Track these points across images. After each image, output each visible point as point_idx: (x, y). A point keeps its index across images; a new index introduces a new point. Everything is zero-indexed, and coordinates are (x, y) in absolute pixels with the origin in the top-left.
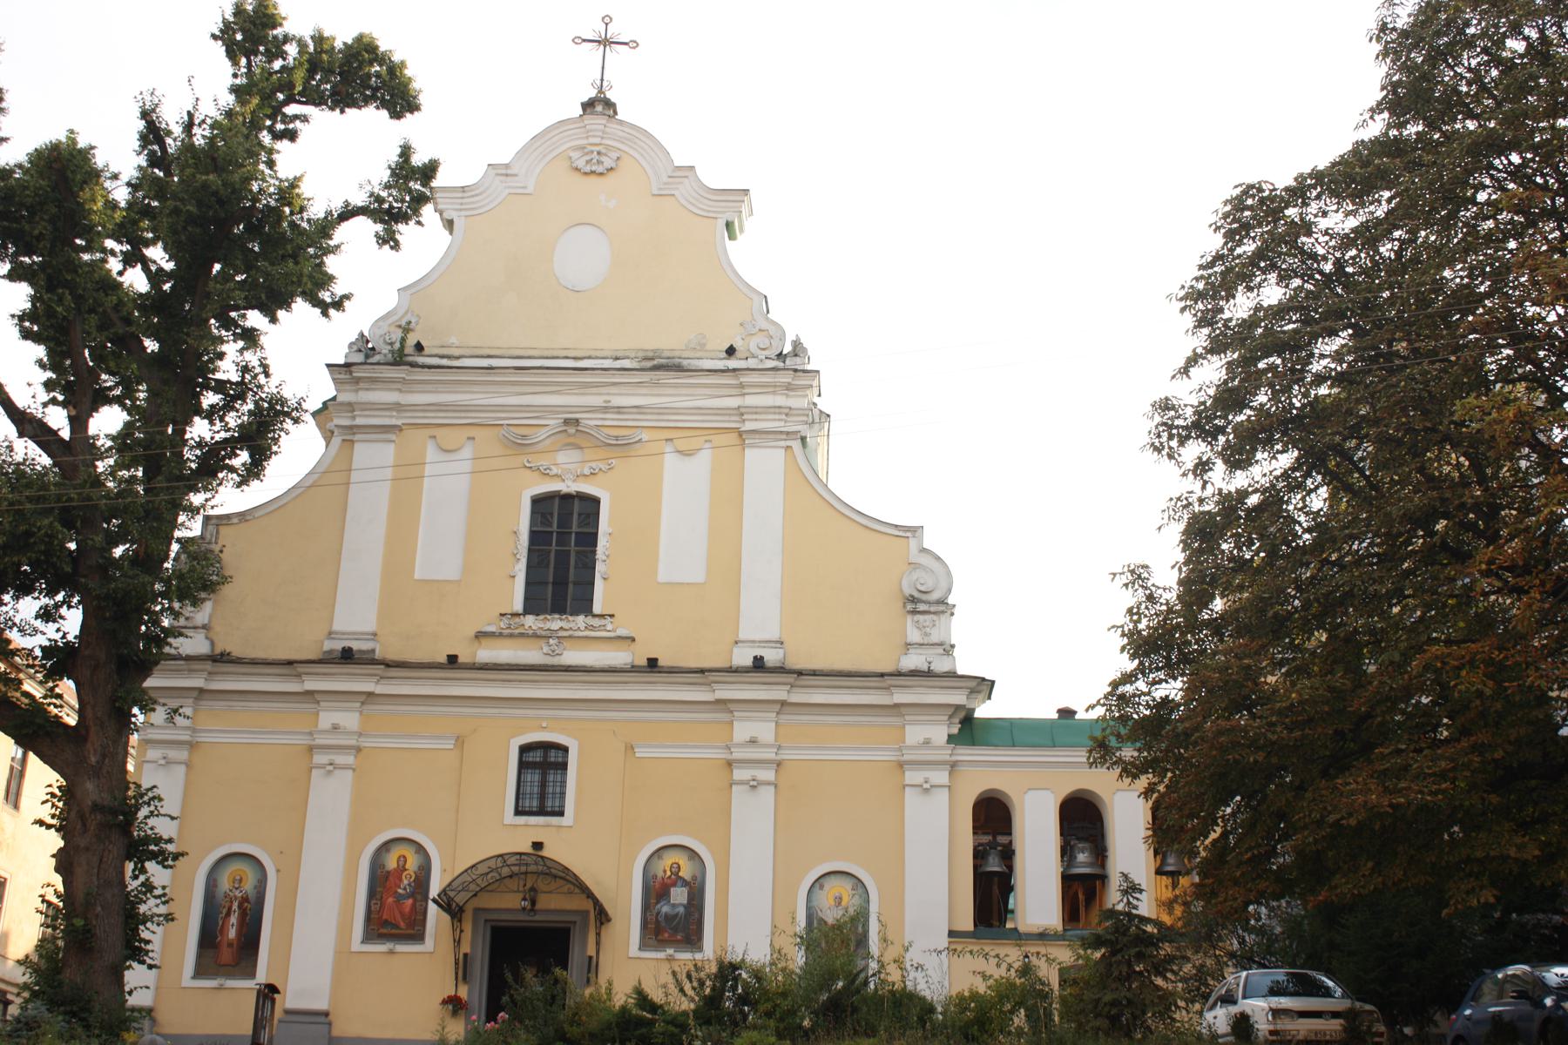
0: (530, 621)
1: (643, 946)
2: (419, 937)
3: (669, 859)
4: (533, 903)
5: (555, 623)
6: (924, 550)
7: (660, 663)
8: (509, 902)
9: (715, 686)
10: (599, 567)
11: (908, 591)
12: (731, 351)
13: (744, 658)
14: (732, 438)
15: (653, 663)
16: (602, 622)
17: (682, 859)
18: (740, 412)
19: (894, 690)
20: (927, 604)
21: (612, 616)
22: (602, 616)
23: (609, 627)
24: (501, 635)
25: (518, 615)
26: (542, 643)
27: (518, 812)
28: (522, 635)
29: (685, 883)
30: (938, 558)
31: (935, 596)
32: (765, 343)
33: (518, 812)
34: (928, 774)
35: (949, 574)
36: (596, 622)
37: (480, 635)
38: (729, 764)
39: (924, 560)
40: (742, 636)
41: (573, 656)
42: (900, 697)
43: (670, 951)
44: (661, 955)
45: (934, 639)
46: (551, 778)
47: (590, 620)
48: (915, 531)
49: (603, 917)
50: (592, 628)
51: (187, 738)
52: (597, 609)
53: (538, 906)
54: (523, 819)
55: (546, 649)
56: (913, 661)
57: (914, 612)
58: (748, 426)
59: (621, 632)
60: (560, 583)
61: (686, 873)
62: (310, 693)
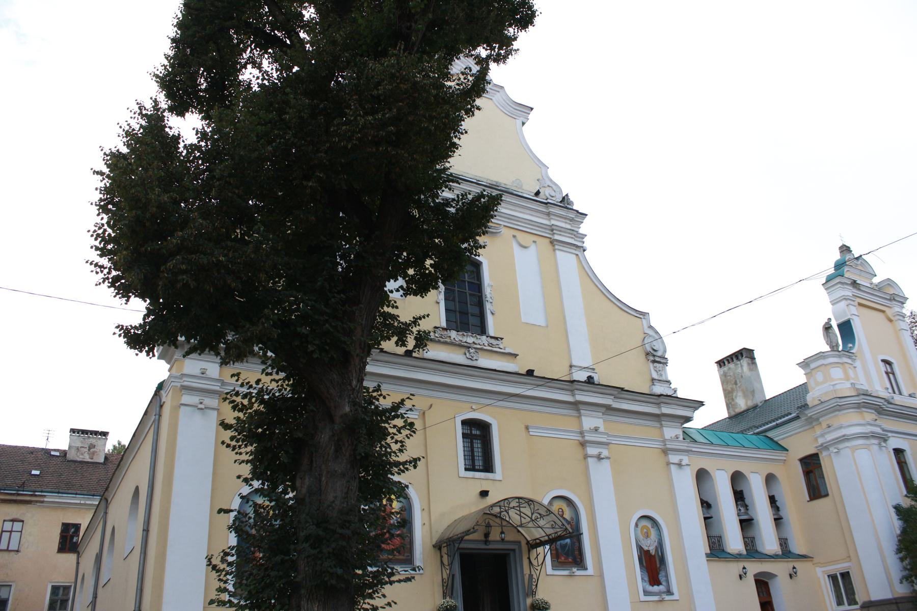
0: (453, 334)
1: (554, 567)
5: (470, 340)
6: (651, 327)
7: (535, 374)
9: (577, 392)
10: (488, 307)
11: (649, 349)
12: (537, 194)
13: (582, 376)
14: (548, 241)
15: (530, 373)
17: (563, 505)
18: (552, 229)
19: (662, 405)
20: (656, 358)
22: (496, 338)
24: (439, 342)
25: (444, 329)
26: (463, 350)
27: (466, 469)
28: (446, 343)
30: (657, 333)
31: (659, 354)
32: (553, 194)
33: (466, 469)
34: (681, 457)
35: (663, 342)
38: (583, 444)
39: (651, 332)
40: (574, 363)
41: (484, 361)
42: (666, 410)
43: (574, 570)
44: (566, 573)
45: (663, 378)
46: (476, 445)
48: (644, 315)
50: (490, 345)
51: (218, 388)
52: (491, 331)
54: (471, 474)
55: (468, 355)
56: (658, 389)
57: (654, 362)
58: (556, 237)
59: (507, 351)
60: (464, 313)
61: (568, 515)
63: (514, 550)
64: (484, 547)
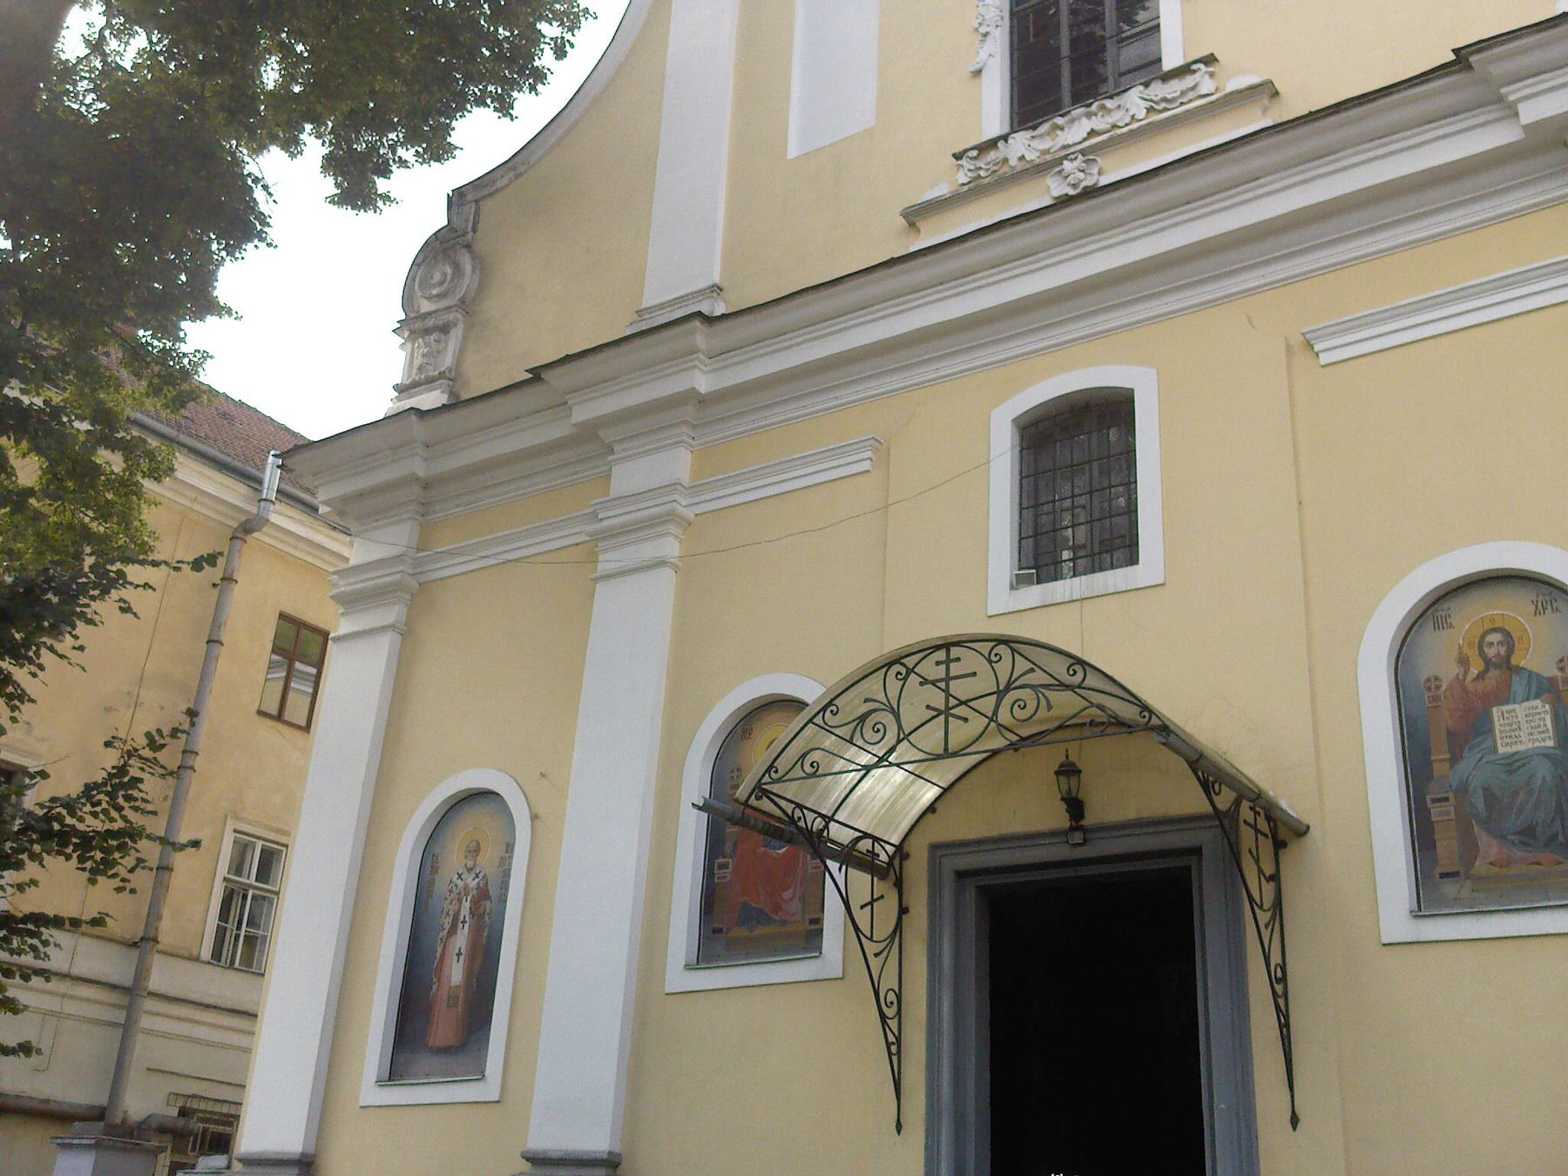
0: (1023, 147)
2: (809, 939)
3: (1469, 616)
4: (1075, 807)
5: (1076, 128)
8: (1025, 810)
9: (1512, 93)
16: (1189, 81)
17: (1512, 608)
21: (1210, 60)
22: (1184, 70)
23: (1207, 86)
25: (992, 144)
29: (1544, 688)
36: (1174, 87)
37: (914, 216)
47: (1159, 90)
49: (1283, 833)
53: (1090, 820)
54: (1034, 594)
62: (589, 434)
63: (1197, 851)
64: (1061, 852)
